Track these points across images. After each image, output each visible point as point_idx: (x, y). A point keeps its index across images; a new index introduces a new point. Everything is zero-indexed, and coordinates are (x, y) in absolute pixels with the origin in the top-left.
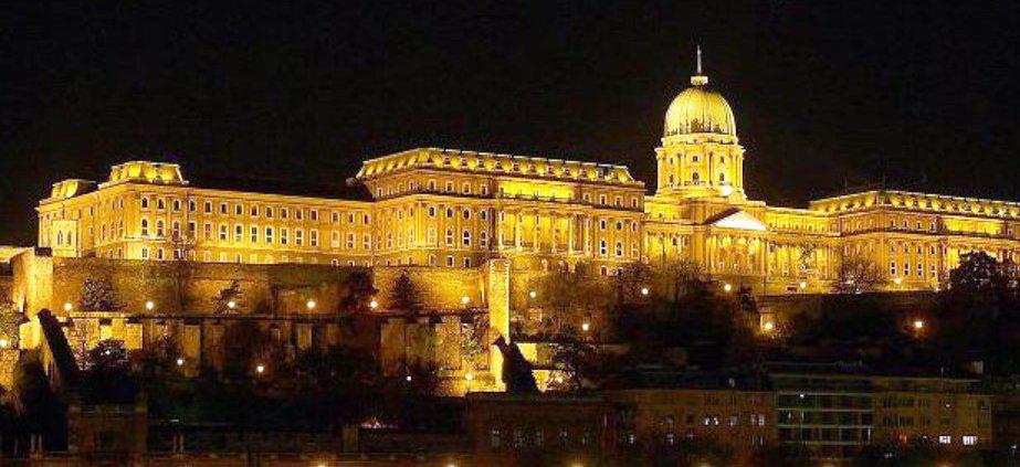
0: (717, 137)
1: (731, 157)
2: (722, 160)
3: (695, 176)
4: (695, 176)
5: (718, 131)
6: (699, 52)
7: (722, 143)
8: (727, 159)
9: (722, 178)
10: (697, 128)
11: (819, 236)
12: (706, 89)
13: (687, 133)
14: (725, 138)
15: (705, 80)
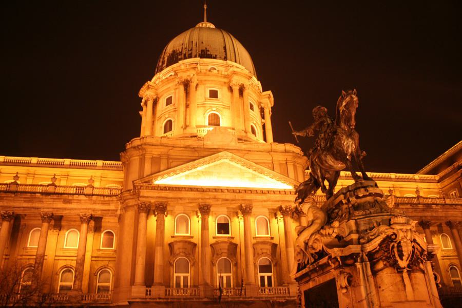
1: (231, 89)
2: (214, 94)
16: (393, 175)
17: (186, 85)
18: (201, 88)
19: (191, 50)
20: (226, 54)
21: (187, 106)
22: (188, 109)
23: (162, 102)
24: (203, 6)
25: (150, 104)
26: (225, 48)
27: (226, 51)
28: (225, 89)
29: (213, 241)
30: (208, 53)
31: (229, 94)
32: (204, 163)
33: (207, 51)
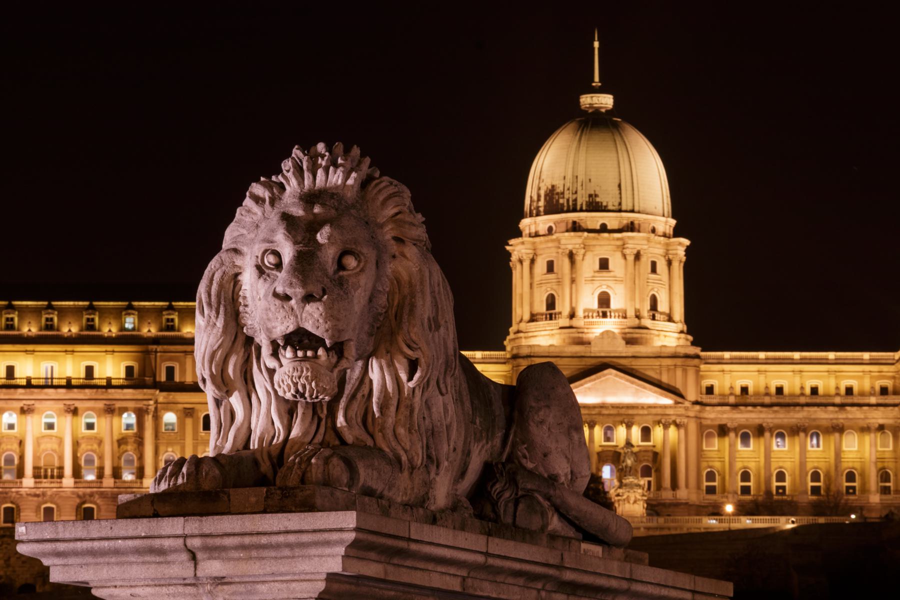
0: (594, 219)
1: (624, 256)
2: (604, 265)
3: (551, 303)
4: (551, 303)
5: (594, 206)
6: (596, 44)
7: (604, 229)
8: (616, 262)
9: (604, 300)
10: (553, 204)
11: (842, 406)
12: (595, 122)
13: (538, 215)
14: (612, 220)
15: (606, 101)
16: (831, 355)
17: (571, 256)
18: (589, 256)
19: (576, 193)
20: (621, 198)
21: (573, 281)
22: (574, 286)
23: (541, 266)
24: (593, 44)
25: (526, 264)
26: (620, 186)
27: (620, 193)
28: (619, 255)
29: (600, 449)
30: (598, 199)
31: (622, 261)
32: (590, 381)
33: (596, 196)
